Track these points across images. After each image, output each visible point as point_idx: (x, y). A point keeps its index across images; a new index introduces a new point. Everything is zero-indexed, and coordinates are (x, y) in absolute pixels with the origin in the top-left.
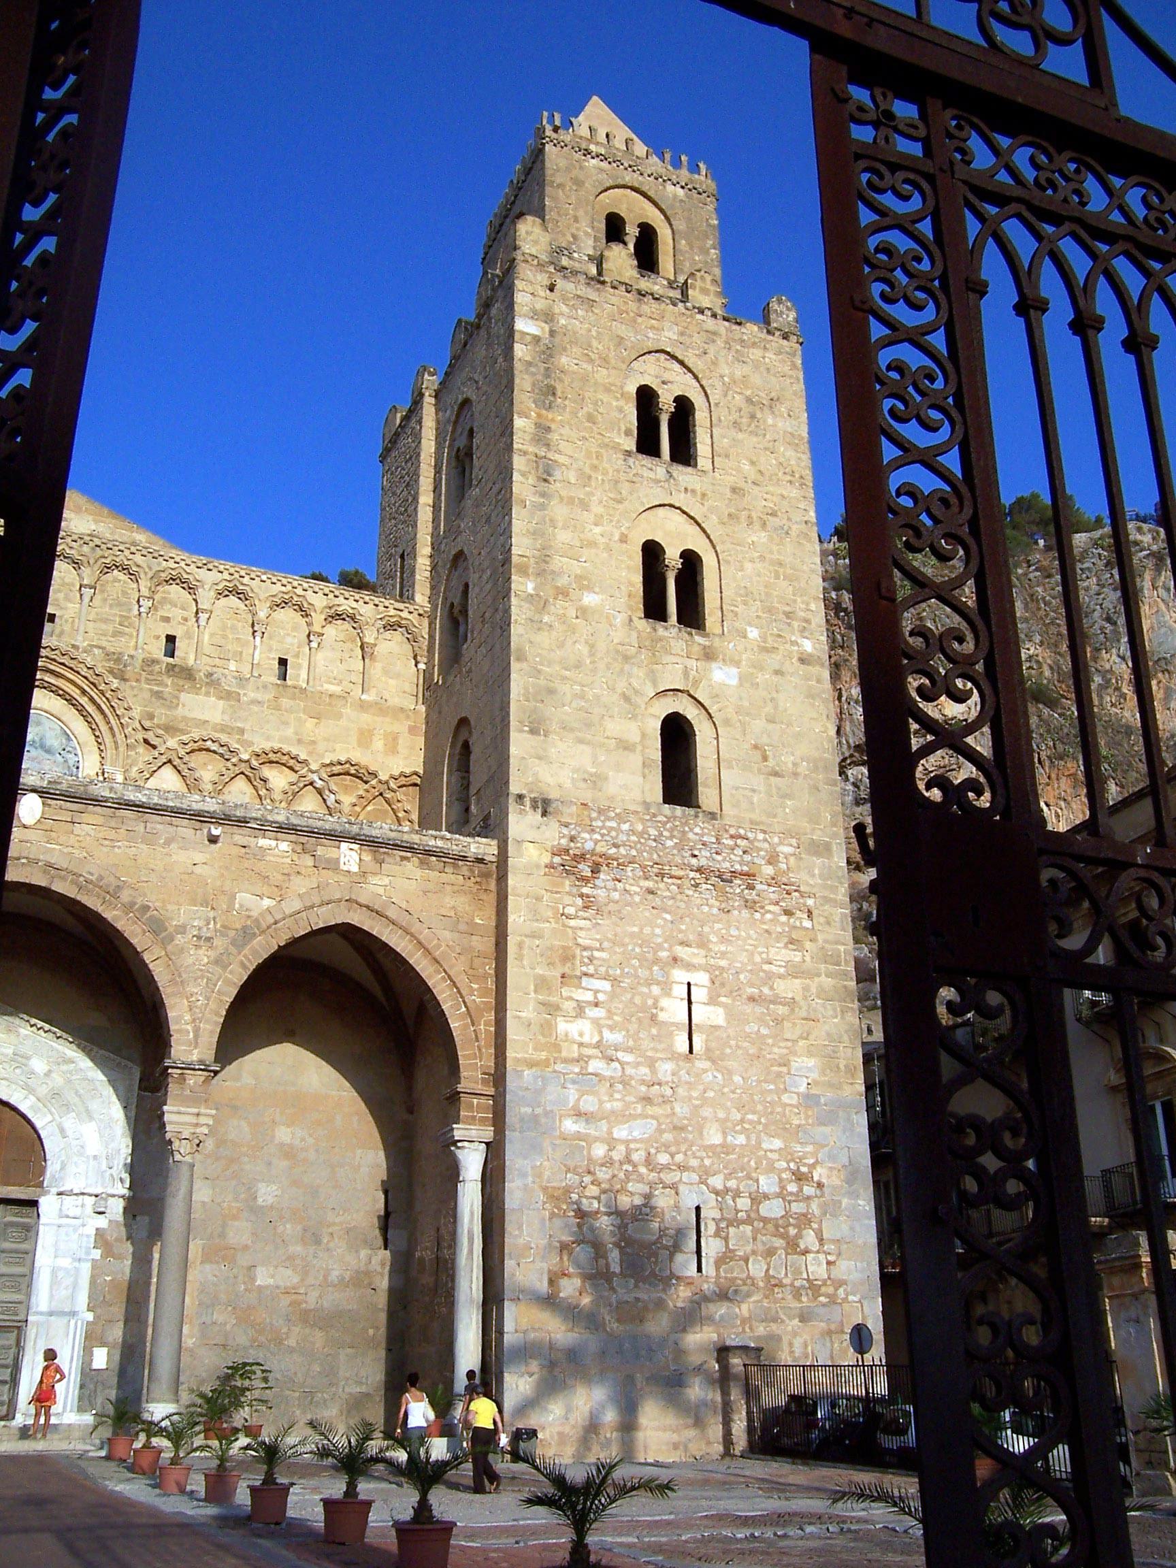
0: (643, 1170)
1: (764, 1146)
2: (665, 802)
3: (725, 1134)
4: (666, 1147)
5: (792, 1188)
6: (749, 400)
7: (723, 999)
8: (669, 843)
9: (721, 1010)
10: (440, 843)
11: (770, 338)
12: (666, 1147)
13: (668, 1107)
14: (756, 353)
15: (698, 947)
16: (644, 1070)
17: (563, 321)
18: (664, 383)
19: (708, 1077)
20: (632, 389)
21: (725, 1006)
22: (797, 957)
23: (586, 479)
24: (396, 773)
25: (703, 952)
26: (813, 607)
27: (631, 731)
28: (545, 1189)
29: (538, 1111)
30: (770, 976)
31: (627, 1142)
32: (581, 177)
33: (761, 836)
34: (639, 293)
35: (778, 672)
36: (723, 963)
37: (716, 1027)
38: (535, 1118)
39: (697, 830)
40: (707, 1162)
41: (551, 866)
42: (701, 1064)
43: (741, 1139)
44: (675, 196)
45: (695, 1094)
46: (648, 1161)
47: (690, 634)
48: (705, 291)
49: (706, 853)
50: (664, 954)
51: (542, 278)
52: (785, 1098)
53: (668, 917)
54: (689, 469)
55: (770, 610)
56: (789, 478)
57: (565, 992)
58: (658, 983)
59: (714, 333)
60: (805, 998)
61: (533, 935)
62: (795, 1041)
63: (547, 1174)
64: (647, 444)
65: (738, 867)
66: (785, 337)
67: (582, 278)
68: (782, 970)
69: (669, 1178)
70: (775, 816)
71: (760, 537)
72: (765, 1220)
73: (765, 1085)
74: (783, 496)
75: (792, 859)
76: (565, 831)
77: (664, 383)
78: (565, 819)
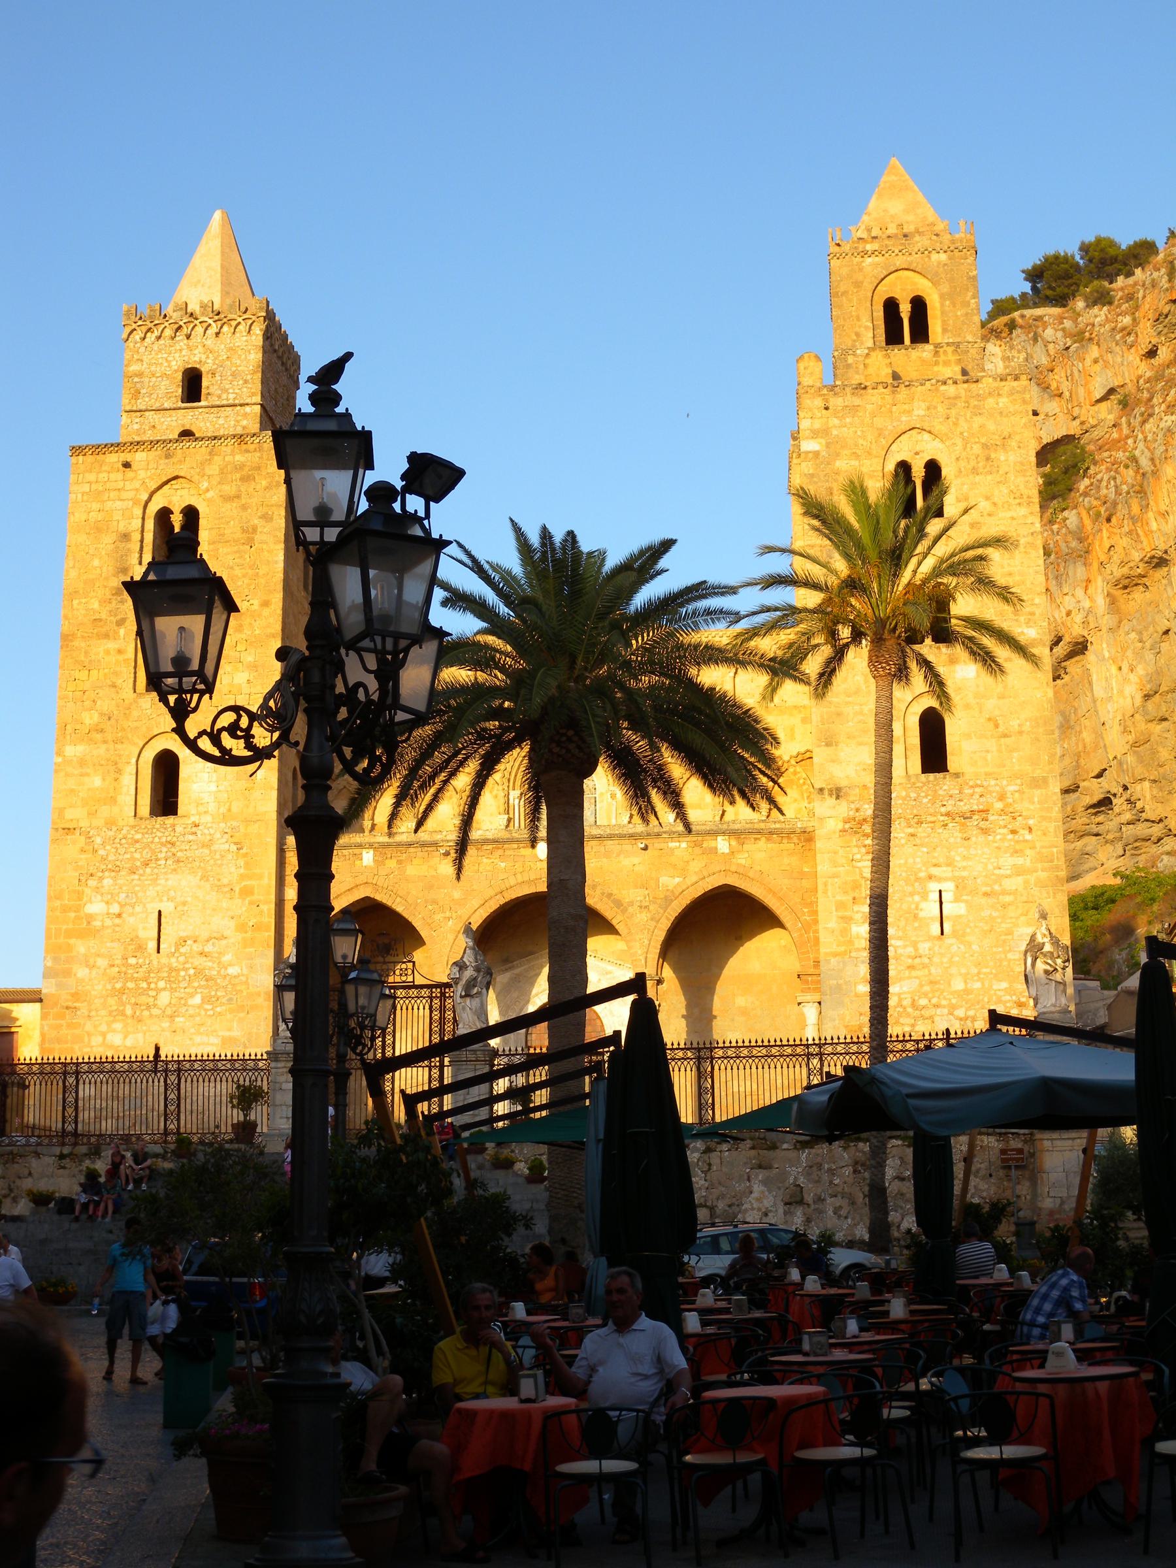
0: (910, 1010)
1: (995, 987)
2: (924, 772)
3: (965, 982)
4: (926, 995)
6: (985, 446)
7: (965, 897)
8: (925, 800)
9: (963, 905)
10: (778, 826)
11: (1003, 383)
12: (926, 995)
13: (926, 971)
14: (991, 402)
15: (948, 865)
16: (910, 950)
17: (835, 432)
18: (917, 453)
19: (954, 949)
20: (891, 467)
21: (966, 901)
22: (1020, 861)
24: (795, 754)
25: (950, 869)
28: (846, 1027)
29: (841, 982)
31: (899, 995)
32: (861, 278)
33: (993, 782)
36: (965, 874)
37: (960, 917)
38: (839, 987)
39: (945, 787)
40: (954, 1001)
42: (952, 941)
43: (977, 985)
44: (939, 263)
45: (945, 960)
46: (914, 1005)
47: (939, 648)
48: (947, 363)
49: (951, 802)
50: (922, 875)
51: (819, 402)
52: (1010, 956)
53: (925, 850)
56: (1018, 501)
57: (856, 908)
58: (919, 893)
59: (957, 397)
60: (1025, 888)
61: (835, 876)
62: (1017, 918)
63: (848, 1018)
65: (975, 808)
66: (1016, 378)
67: (848, 390)
68: (1008, 872)
69: (926, 1013)
70: (1004, 766)
73: (995, 949)
74: (1013, 518)
75: (1017, 795)
76: (853, 806)
77: (917, 453)
78: (851, 799)
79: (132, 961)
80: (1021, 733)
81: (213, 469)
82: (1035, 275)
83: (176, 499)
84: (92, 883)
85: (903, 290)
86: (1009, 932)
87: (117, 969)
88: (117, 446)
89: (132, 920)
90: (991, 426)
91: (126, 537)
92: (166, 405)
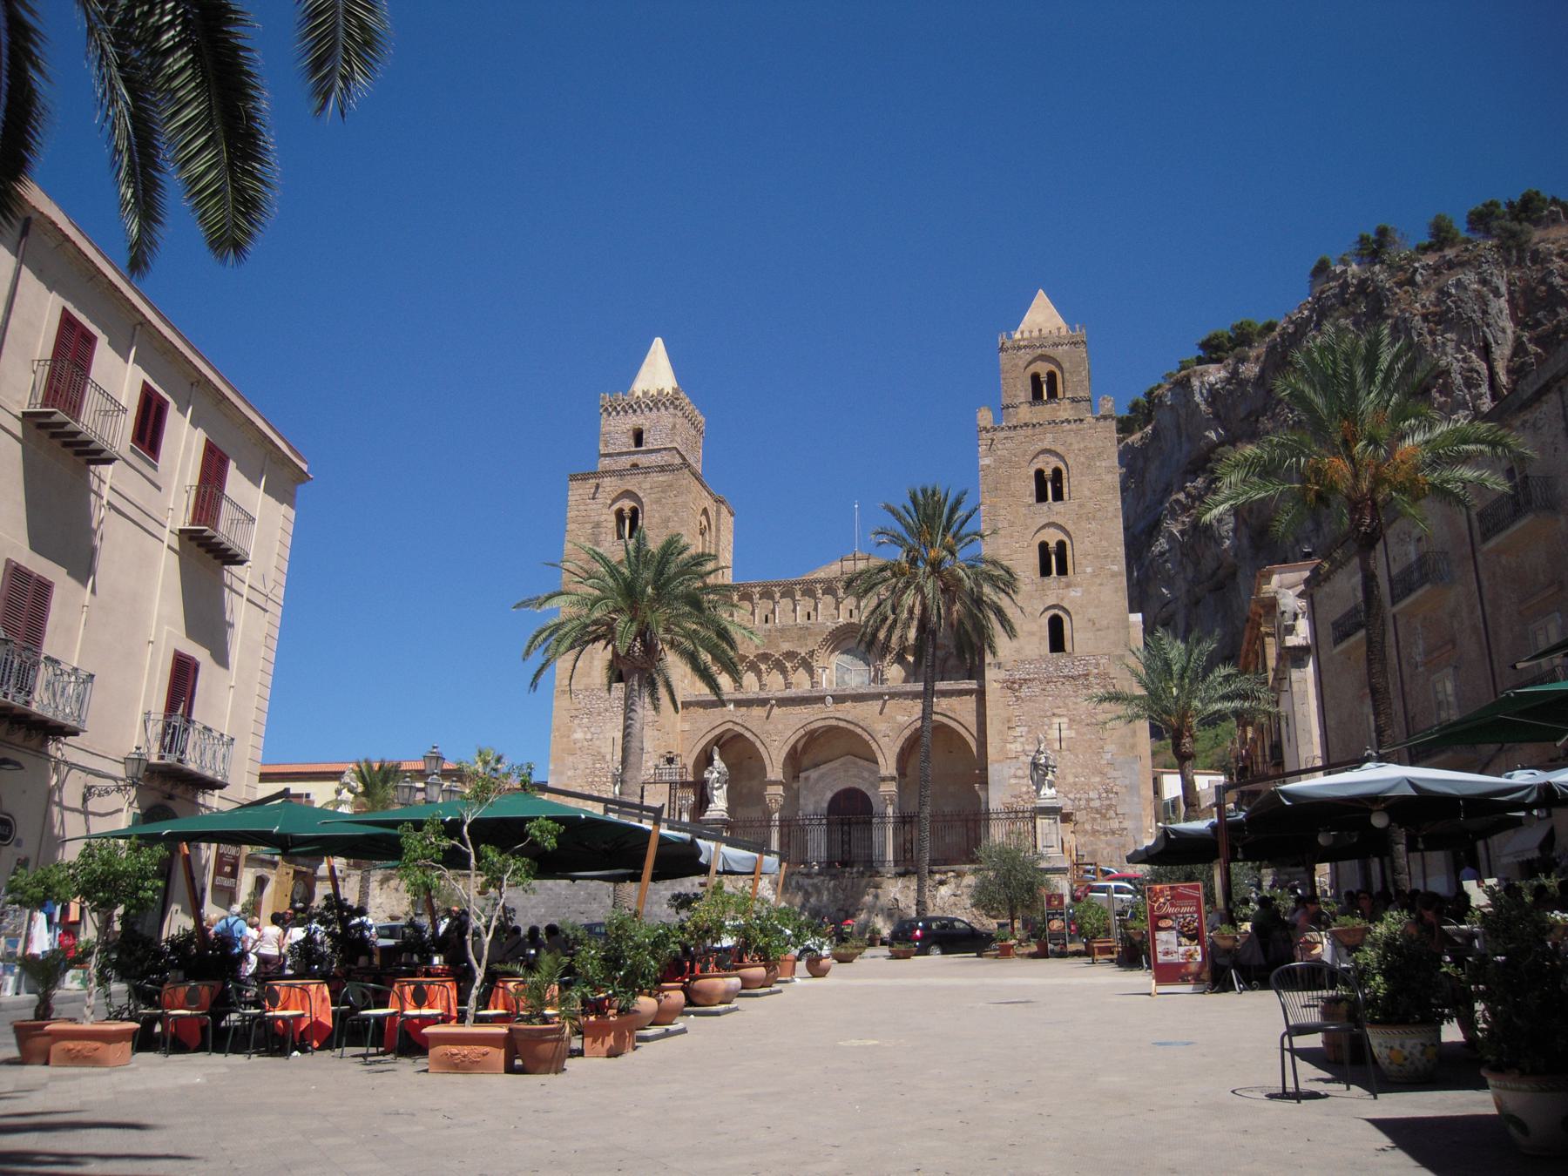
5: (1105, 795)
23: (1012, 524)
26: (1118, 549)
27: (1035, 628)
30: (1095, 714)
34: (1034, 426)
35: (1101, 585)
41: (1002, 688)
48: (1065, 410)
54: (1059, 502)
55: (1098, 557)
59: (1070, 431)
64: (1041, 497)
71: (1093, 526)
72: (1092, 808)
79: (598, 766)
80: (1108, 628)
81: (647, 485)
82: (1205, 345)
83: (627, 504)
84: (577, 721)
85: (1043, 369)
86: (1102, 748)
87: (588, 771)
88: (596, 475)
89: (598, 742)
90: (1093, 445)
91: (597, 525)
92: (625, 450)
